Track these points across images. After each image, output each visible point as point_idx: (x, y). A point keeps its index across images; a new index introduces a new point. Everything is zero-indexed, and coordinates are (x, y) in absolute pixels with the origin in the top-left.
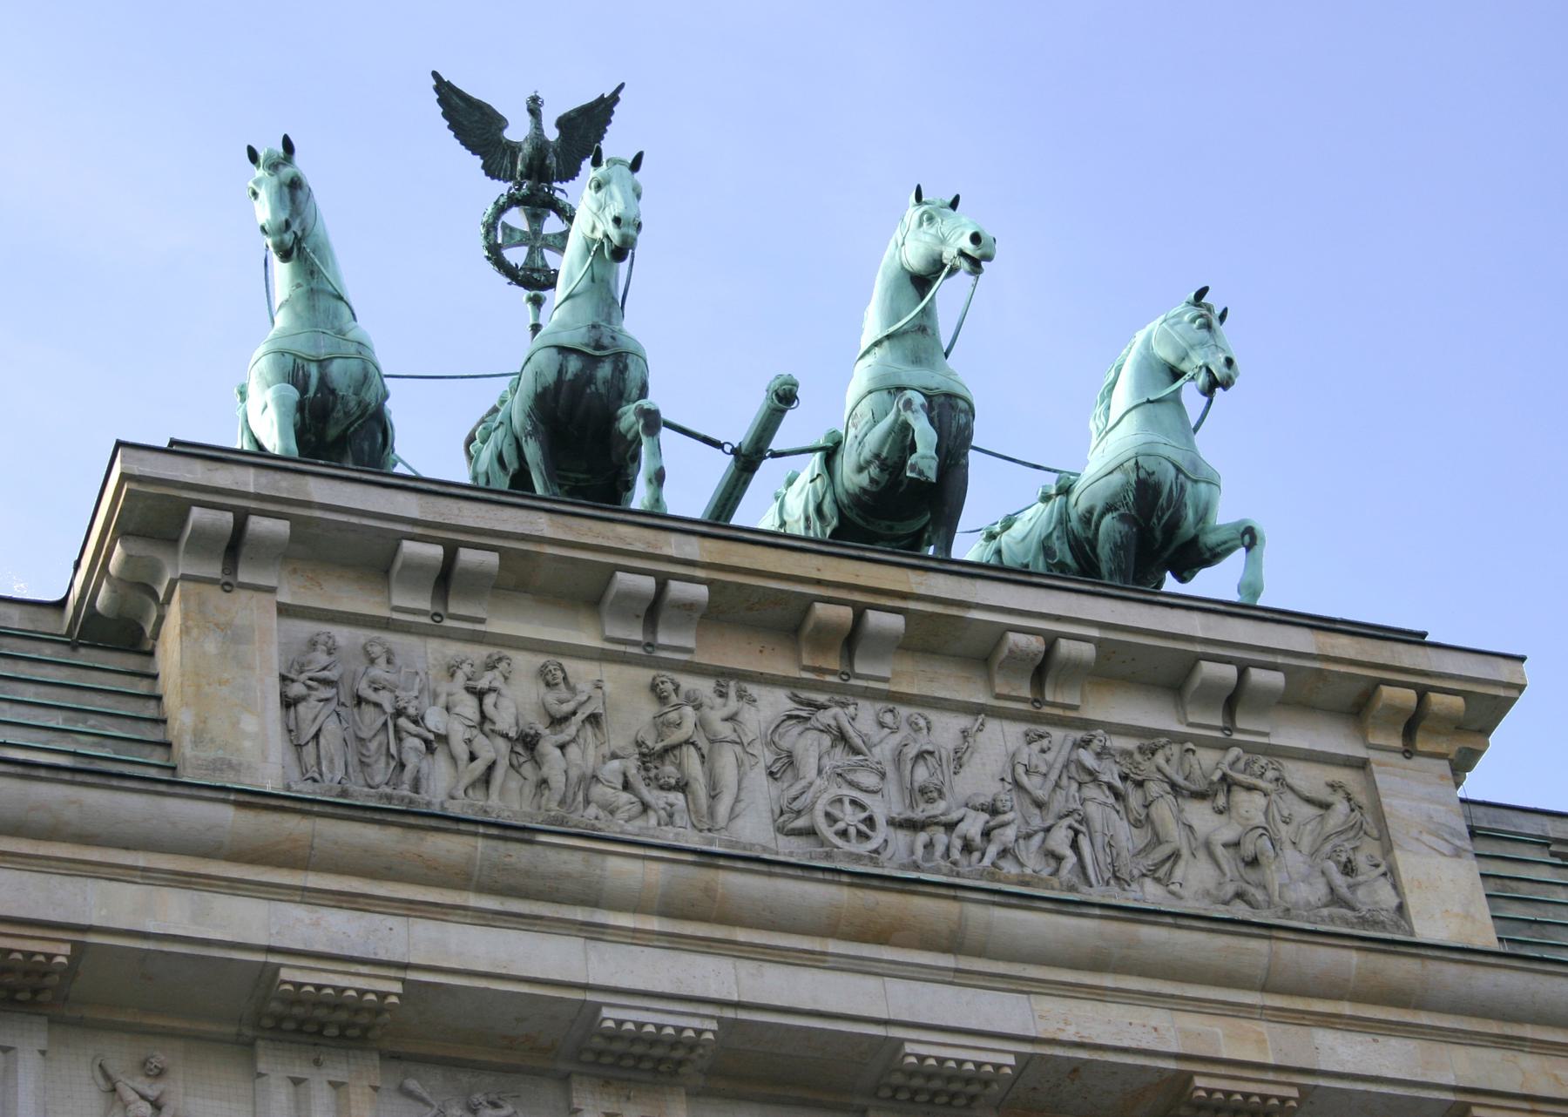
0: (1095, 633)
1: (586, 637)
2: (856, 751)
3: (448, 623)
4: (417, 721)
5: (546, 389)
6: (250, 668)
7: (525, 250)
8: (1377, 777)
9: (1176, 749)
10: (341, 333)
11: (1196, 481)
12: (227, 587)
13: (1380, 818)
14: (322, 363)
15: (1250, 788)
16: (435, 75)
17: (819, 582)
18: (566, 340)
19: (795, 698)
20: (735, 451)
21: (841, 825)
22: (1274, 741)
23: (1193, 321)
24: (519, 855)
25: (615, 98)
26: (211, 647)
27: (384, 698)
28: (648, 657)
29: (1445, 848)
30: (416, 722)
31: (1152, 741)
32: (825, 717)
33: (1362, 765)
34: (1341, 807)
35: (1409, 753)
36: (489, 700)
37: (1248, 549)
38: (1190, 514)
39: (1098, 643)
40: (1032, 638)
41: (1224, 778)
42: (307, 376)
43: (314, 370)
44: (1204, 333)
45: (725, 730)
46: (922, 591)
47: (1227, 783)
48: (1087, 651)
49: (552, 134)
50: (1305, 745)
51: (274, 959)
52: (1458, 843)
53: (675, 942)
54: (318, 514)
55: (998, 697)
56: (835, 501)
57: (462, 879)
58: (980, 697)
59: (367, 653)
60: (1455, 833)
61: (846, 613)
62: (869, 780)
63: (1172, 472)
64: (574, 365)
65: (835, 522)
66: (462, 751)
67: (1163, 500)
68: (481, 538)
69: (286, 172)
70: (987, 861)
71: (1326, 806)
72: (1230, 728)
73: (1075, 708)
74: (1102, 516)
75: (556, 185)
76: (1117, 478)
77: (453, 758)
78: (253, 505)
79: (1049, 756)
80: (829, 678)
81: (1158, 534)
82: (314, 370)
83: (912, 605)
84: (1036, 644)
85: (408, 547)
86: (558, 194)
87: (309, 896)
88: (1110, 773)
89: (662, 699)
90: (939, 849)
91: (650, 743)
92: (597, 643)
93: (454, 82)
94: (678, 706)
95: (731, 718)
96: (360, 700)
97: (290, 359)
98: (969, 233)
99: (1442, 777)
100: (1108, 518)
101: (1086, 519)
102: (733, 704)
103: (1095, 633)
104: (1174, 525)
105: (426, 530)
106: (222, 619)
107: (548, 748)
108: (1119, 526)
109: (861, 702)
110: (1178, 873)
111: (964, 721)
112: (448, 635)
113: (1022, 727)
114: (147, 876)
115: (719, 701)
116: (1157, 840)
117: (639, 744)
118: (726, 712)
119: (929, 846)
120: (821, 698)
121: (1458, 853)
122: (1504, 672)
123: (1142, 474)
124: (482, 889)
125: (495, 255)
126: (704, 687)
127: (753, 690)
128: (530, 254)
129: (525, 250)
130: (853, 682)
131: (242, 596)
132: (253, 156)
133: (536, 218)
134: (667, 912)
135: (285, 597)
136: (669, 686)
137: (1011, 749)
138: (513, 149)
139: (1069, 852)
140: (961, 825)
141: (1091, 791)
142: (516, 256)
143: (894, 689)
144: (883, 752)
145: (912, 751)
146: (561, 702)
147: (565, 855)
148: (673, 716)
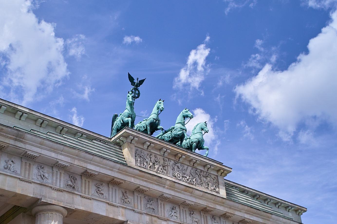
1: (159, 153)
2: (179, 169)
4: (145, 160)
5: (152, 122)
6: (133, 152)
8: (218, 177)
12: (131, 143)
13: (218, 182)
14: (132, 115)
15: (209, 177)
16: (128, 73)
17: (179, 152)
18: (154, 118)
19: (174, 162)
20: (165, 131)
21: (178, 176)
24: (160, 179)
25: (145, 79)
27: (143, 157)
30: (145, 160)
31: (201, 171)
32: (177, 165)
33: (217, 176)
34: (215, 180)
36: (151, 158)
39: (200, 161)
41: (207, 176)
43: (131, 115)
44: (206, 127)
45: (169, 164)
47: (207, 176)
49: (138, 82)
50: (213, 173)
51: (140, 186)
53: (170, 189)
55: (190, 164)
56: (172, 137)
57: (155, 181)
58: (189, 164)
59: (141, 152)
62: (180, 171)
65: (171, 139)
67: (200, 143)
70: (189, 182)
71: (214, 180)
72: (208, 171)
73: (196, 167)
74: (194, 143)
76: (196, 140)
77: (148, 164)
79: (193, 171)
81: (199, 146)
87: (143, 180)
88: (198, 174)
89: (164, 160)
90: (185, 180)
91: (163, 165)
95: (169, 163)
96: (141, 157)
97: (128, 114)
98: (191, 115)
100: (195, 143)
101: (192, 142)
102: (170, 162)
103: (200, 161)
104: (201, 145)
105: (149, 141)
106: (130, 146)
107: (155, 164)
108: (196, 144)
110: (203, 185)
111: (187, 166)
112: (148, 151)
113: (191, 168)
114: (131, 176)
115: (168, 161)
116: (201, 181)
117: (162, 165)
118: (169, 163)
119: (184, 179)
120: (176, 162)
121: (224, 186)
122: (230, 170)
124: (156, 182)
126: (167, 159)
127: (171, 160)
128: (134, 94)
131: (132, 144)
132: (129, 92)
134: (170, 187)
135: (135, 145)
137: (191, 170)
138: (135, 83)
139: (195, 181)
140: (187, 178)
141: (197, 175)
144: (181, 169)
145: (183, 169)
147: (164, 180)
148: (165, 163)
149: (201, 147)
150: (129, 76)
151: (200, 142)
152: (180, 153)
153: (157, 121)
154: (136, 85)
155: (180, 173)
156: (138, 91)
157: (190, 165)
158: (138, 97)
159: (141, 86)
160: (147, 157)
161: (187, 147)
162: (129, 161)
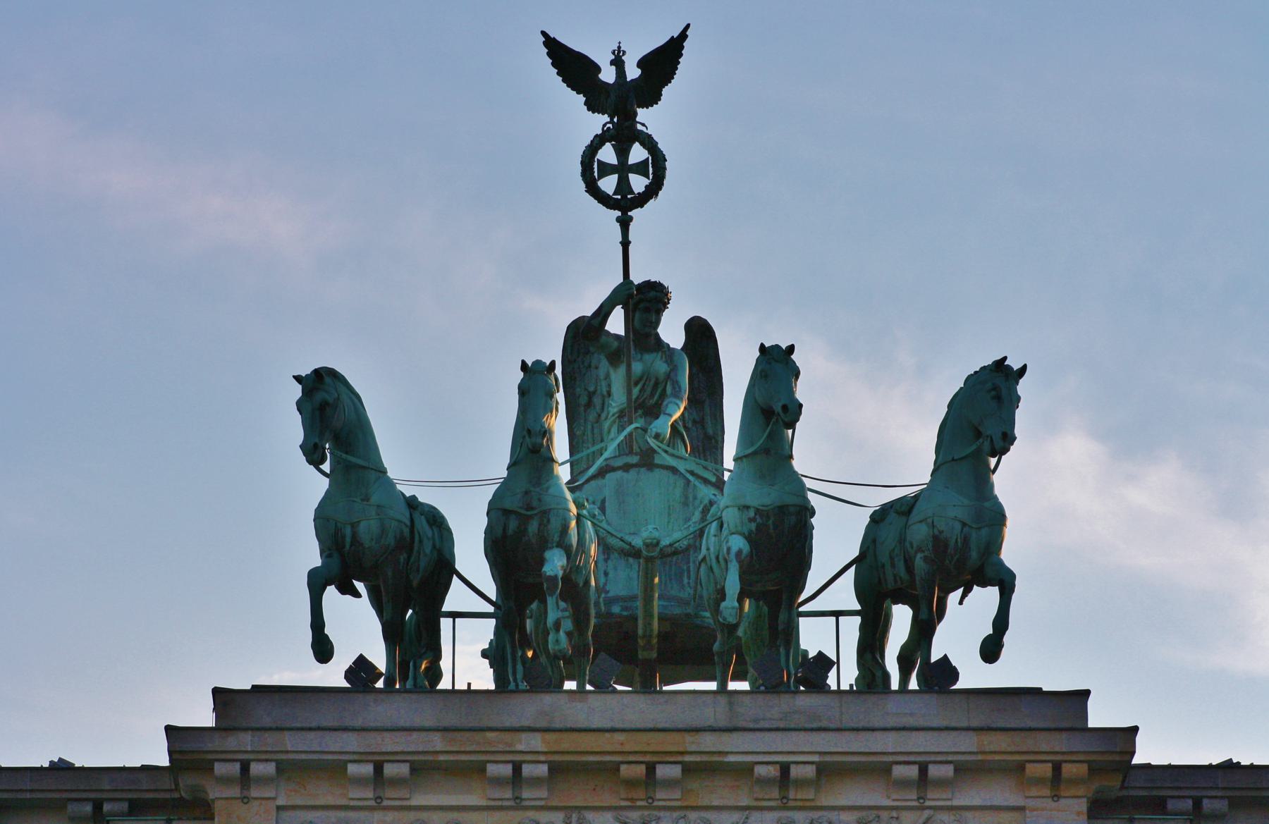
0: (816, 758)
3: (385, 803)
9: (885, 815)
11: (979, 528)
12: (245, 800)
16: (543, 33)
18: (508, 505)
22: (955, 803)
23: (990, 391)
25: (683, 36)
28: (518, 804)
33: (1021, 809)
35: (1056, 797)
38: (974, 554)
40: (771, 768)
42: (344, 537)
43: (348, 531)
46: (693, 748)
48: (810, 771)
49: (633, 73)
54: (292, 756)
55: (757, 799)
61: (641, 769)
63: (958, 526)
64: (513, 525)
68: (396, 757)
69: (319, 396)
75: (643, 115)
78: (251, 756)
80: (639, 803)
82: (348, 531)
83: (688, 758)
84: (773, 771)
85: (352, 769)
86: (639, 127)
92: (484, 803)
93: (558, 38)
98: (780, 404)
99: (1079, 814)
100: (919, 555)
109: (662, 814)
123: (936, 532)
125: (593, 189)
130: (656, 803)
131: (256, 803)
133: (622, 152)
135: (280, 802)
142: (608, 184)
143: (685, 804)
149: (983, 565)
150: (548, 54)
151: (946, 546)
152: (631, 758)
153: (529, 518)
154: (623, 96)
156: (649, 143)
157: (755, 804)
158: (653, 191)
159: (665, 91)
161: (896, 581)
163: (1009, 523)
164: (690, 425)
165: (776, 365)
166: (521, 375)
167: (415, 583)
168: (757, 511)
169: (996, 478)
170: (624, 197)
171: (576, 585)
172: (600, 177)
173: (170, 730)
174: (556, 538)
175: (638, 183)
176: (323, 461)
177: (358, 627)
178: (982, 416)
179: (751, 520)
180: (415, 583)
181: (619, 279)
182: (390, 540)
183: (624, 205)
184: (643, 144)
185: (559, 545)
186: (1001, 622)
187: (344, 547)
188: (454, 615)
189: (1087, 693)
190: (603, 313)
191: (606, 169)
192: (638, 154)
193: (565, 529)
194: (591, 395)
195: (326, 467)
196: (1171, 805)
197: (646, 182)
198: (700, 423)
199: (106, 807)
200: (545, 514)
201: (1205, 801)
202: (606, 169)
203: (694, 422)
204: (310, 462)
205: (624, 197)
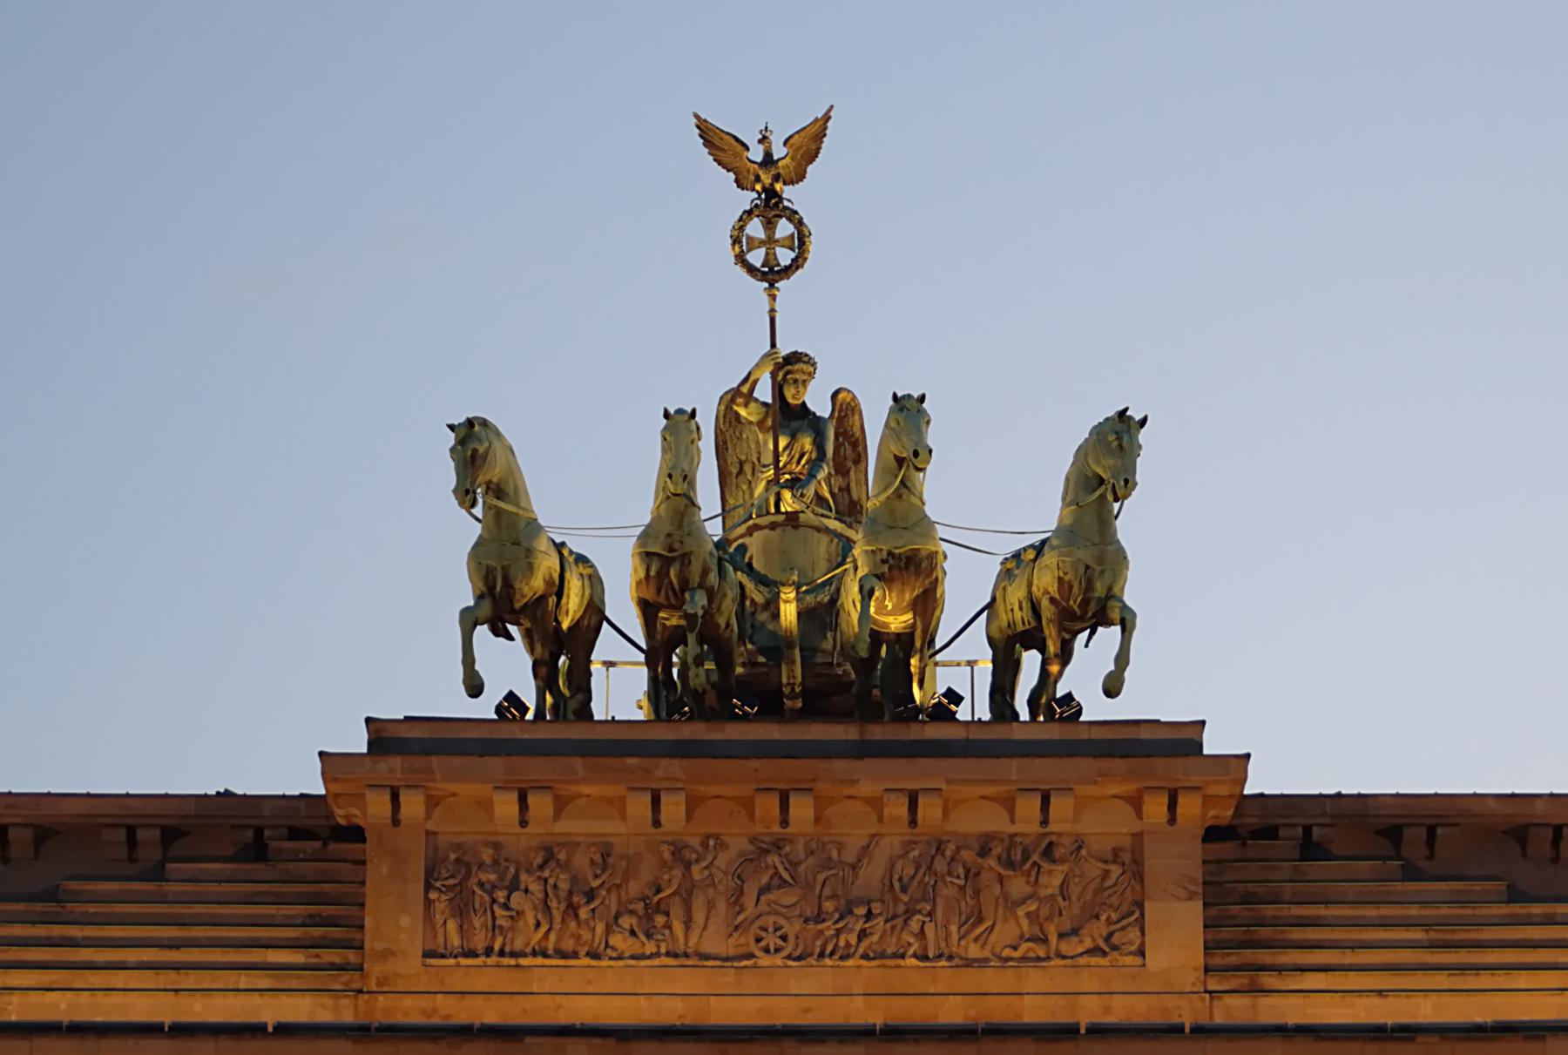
7: (762, 251)
10: (518, 544)
11: (1103, 572)
16: (697, 116)
25: (827, 118)
26: (384, 870)
29: (1182, 893)
30: (506, 907)
36: (551, 881)
37: (1123, 631)
42: (495, 580)
52: (1193, 888)
60: (1193, 881)
66: (530, 919)
86: (786, 203)
94: (671, 868)
110: (993, 938)
118: (704, 864)
121: (1190, 899)
125: (741, 259)
129: (762, 251)
133: (769, 225)
136: (667, 855)
142: (756, 258)
145: (821, 877)
146: (596, 877)
155: (781, 921)
158: (797, 264)
160: (523, 877)
162: (379, 946)
163: (1131, 566)
164: (836, 490)
165: (909, 410)
166: (664, 421)
167: (565, 626)
168: (890, 553)
169: (1118, 522)
170: (771, 269)
171: (718, 626)
172: (749, 250)
173: (321, 754)
174: (697, 580)
175: (785, 257)
176: (473, 505)
177: (509, 666)
178: (1107, 463)
179: (884, 561)
180: (565, 626)
181: (768, 347)
182: (538, 583)
183: (771, 275)
184: (789, 219)
185: (700, 586)
186: (1122, 659)
187: (495, 587)
188: (609, 664)
189: (1203, 723)
190: (749, 380)
191: (753, 244)
192: (784, 228)
193: (705, 572)
194: (741, 464)
195: (478, 511)
196: (1281, 833)
197: (793, 255)
198: (848, 489)
199: (267, 833)
200: (685, 558)
201: (1315, 829)
202: (753, 244)
203: (840, 489)
204: (461, 504)
205: (771, 269)
